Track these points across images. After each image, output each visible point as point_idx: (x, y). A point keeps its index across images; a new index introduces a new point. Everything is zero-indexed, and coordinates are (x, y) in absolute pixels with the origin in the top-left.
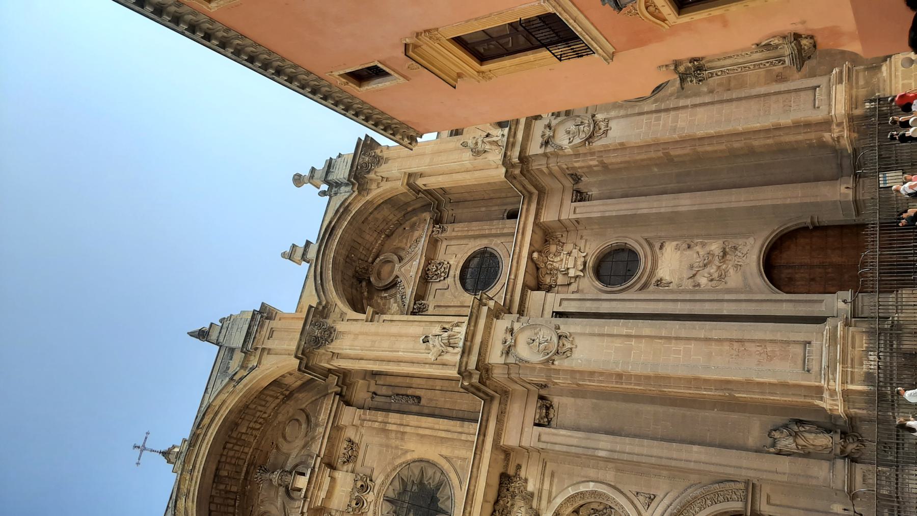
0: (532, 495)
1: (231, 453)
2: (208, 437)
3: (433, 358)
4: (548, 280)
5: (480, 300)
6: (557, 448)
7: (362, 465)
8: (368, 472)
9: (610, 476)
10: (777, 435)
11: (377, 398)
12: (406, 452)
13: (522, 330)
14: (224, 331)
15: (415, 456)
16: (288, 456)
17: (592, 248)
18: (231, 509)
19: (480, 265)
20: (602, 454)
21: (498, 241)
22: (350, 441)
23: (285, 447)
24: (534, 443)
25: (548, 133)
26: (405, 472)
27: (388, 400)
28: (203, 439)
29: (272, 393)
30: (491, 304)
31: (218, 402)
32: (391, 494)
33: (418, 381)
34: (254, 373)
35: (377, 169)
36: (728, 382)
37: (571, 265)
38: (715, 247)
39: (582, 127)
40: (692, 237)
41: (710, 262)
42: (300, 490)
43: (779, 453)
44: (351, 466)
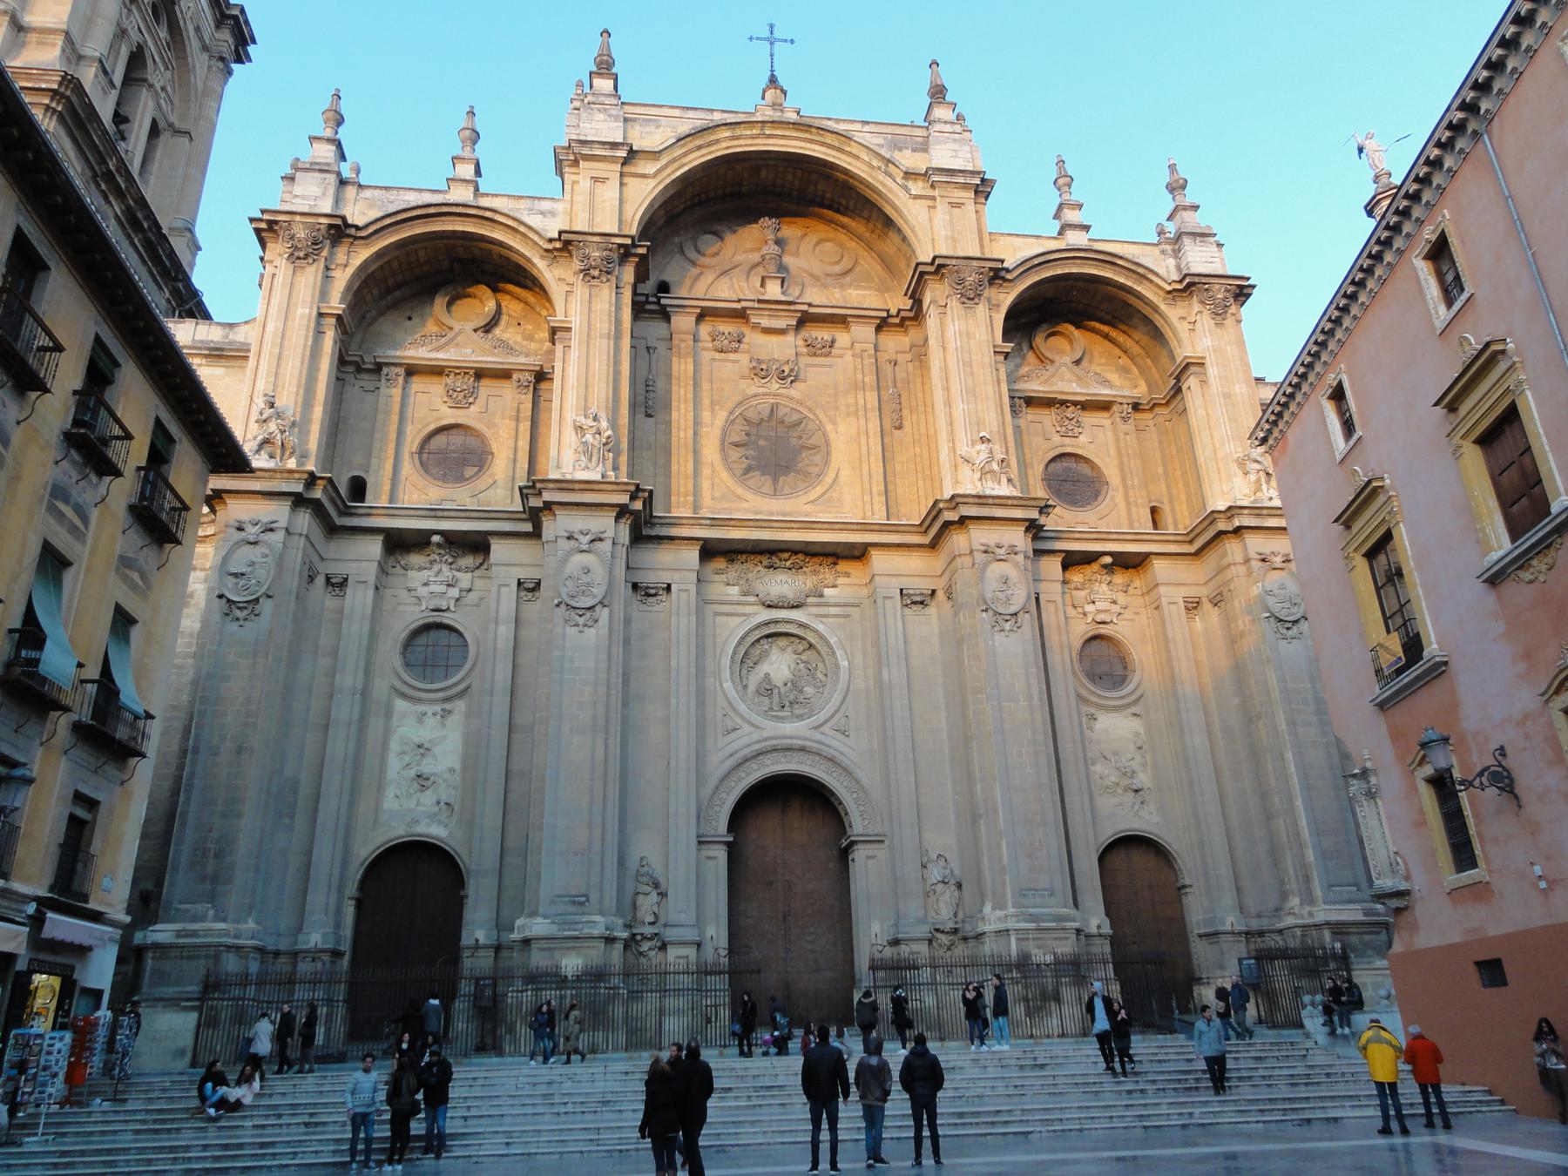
0: (821, 596)
1: (790, 177)
4: (1076, 577)
5: (1047, 506)
6: (881, 621)
7: (807, 365)
8: (802, 375)
10: (942, 862)
11: (889, 368)
12: (834, 422)
13: (1016, 565)
14: (948, 128)
15: (832, 436)
16: (796, 254)
17: (1122, 630)
18: (720, 192)
21: (1120, 499)
22: (833, 342)
23: (806, 246)
24: (881, 592)
25: (1278, 560)
26: (811, 425)
27: (890, 384)
28: (805, 140)
30: (1042, 520)
31: (855, 149)
32: (782, 412)
33: (923, 424)
34: (901, 193)
35: (1206, 313)
36: (995, 811)
37: (1099, 605)
38: (1143, 779)
39: (1287, 605)
41: (1125, 774)
42: (763, 285)
43: (924, 866)
44: (805, 350)
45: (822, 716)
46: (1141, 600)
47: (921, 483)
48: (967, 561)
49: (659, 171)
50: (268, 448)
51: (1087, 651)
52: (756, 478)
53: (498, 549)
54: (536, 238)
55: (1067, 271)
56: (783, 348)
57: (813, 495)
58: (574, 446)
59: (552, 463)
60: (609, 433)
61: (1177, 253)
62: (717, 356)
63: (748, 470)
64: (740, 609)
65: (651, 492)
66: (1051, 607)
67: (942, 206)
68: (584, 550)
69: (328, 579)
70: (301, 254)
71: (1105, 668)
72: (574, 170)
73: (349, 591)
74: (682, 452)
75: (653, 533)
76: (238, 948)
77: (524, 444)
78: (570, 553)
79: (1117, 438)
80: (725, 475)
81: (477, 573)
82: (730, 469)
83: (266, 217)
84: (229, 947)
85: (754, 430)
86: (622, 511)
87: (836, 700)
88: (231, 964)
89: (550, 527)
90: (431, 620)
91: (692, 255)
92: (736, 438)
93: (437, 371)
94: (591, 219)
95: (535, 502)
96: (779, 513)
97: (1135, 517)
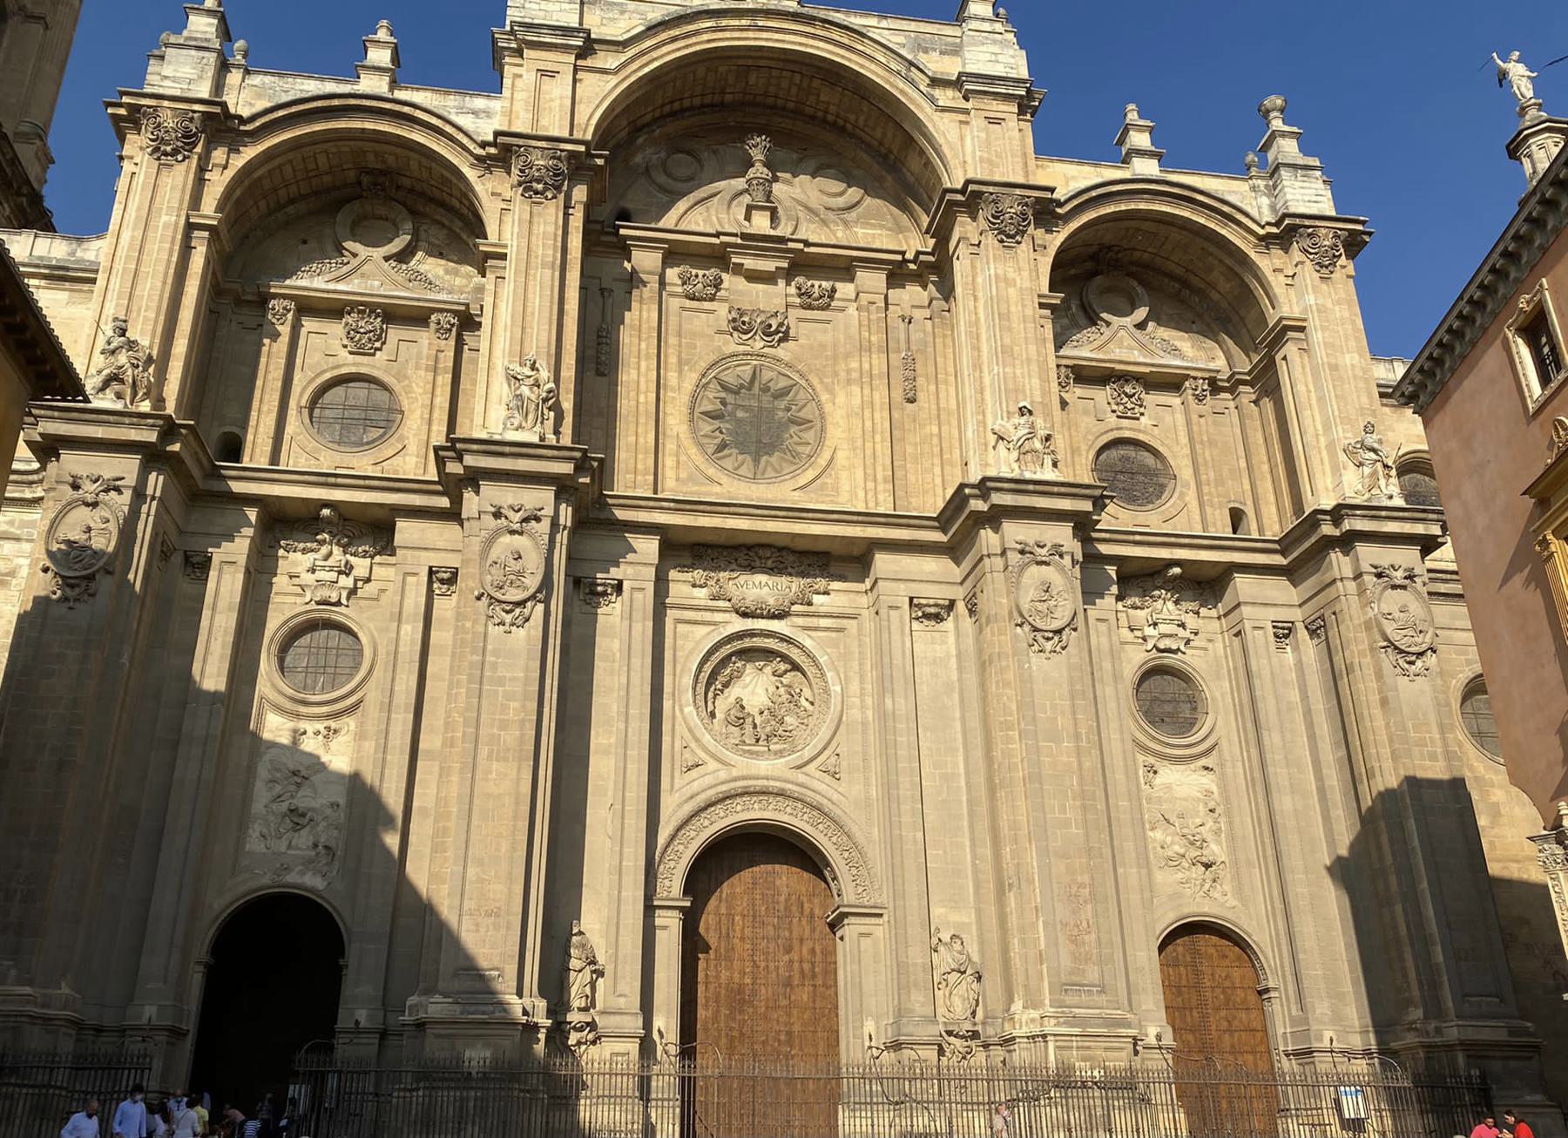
0: (810, 604)
1: (785, 84)
2: (811, 42)
3: (997, 428)
7: (800, 320)
8: (792, 333)
9: (855, 714)
12: (832, 392)
14: (986, 26)
15: (828, 408)
17: (1192, 660)
18: (697, 101)
19: (1150, 473)
20: (888, 701)
22: (834, 290)
26: (802, 394)
29: (890, 135)
32: (767, 375)
37: (1163, 628)
38: (1216, 850)
40: (1228, 813)
42: (748, 218)
45: (807, 753)
46: (1216, 624)
47: (937, 470)
48: (999, 562)
49: (624, 66)
50: (116, 386)
51: (1145, 685)
52: (732, 458)
53: (406, 530)
54: (465, 140)
55: (1132, 206)
56: (773, 298)
57: (802, 481)
58: (505, 400)
59: (478, 420)
60: (551, 385)
61: (1273, 190)
62: (688, 303)
63: (722, 447)
64: (707, 616)
65: (601, 461)
66: (1103, 627)
67: (977, 121)
68: (514, 535)
69: (187, 558)
70: (169, 149)
71: (1168, 708)
72: (518, 61)
73: (213, 574)
74: (642, 420)
75: (603, 516)
76: (47, 1020)
77: (442, 400)
78: (497, 533)
79: (1188, 423)
80: (693, 450)
81: (378, 559)
82: (701, 445)
83: (125, 99)
84: (33, 1018)
85: (730, 398)
86: (563, 488)
87: (824, 733)
88: (35, 1040)
89: (471, 502)
90: (317, 615)
91: (662, 179)
92: (709, 408)
93: (332, 309)
94: (536, 121)
95: (454, 468)
96: (758, 499)
97: (1209, 518)
